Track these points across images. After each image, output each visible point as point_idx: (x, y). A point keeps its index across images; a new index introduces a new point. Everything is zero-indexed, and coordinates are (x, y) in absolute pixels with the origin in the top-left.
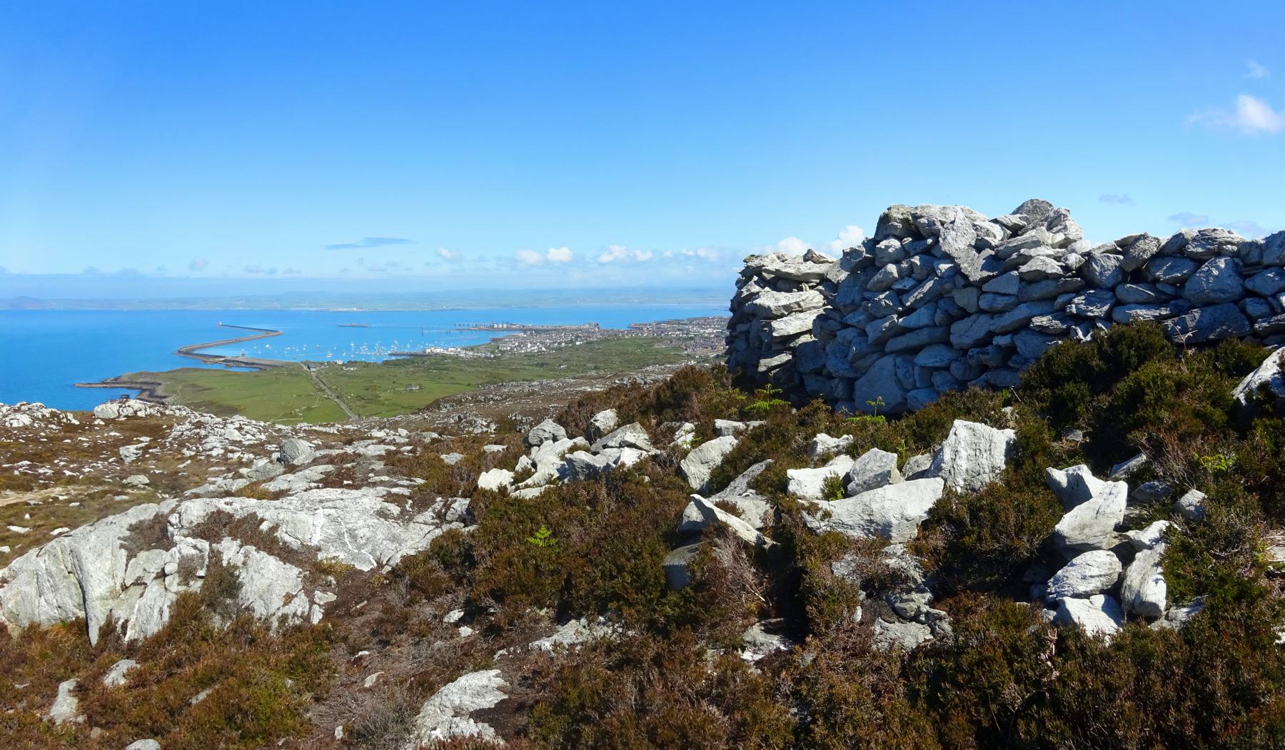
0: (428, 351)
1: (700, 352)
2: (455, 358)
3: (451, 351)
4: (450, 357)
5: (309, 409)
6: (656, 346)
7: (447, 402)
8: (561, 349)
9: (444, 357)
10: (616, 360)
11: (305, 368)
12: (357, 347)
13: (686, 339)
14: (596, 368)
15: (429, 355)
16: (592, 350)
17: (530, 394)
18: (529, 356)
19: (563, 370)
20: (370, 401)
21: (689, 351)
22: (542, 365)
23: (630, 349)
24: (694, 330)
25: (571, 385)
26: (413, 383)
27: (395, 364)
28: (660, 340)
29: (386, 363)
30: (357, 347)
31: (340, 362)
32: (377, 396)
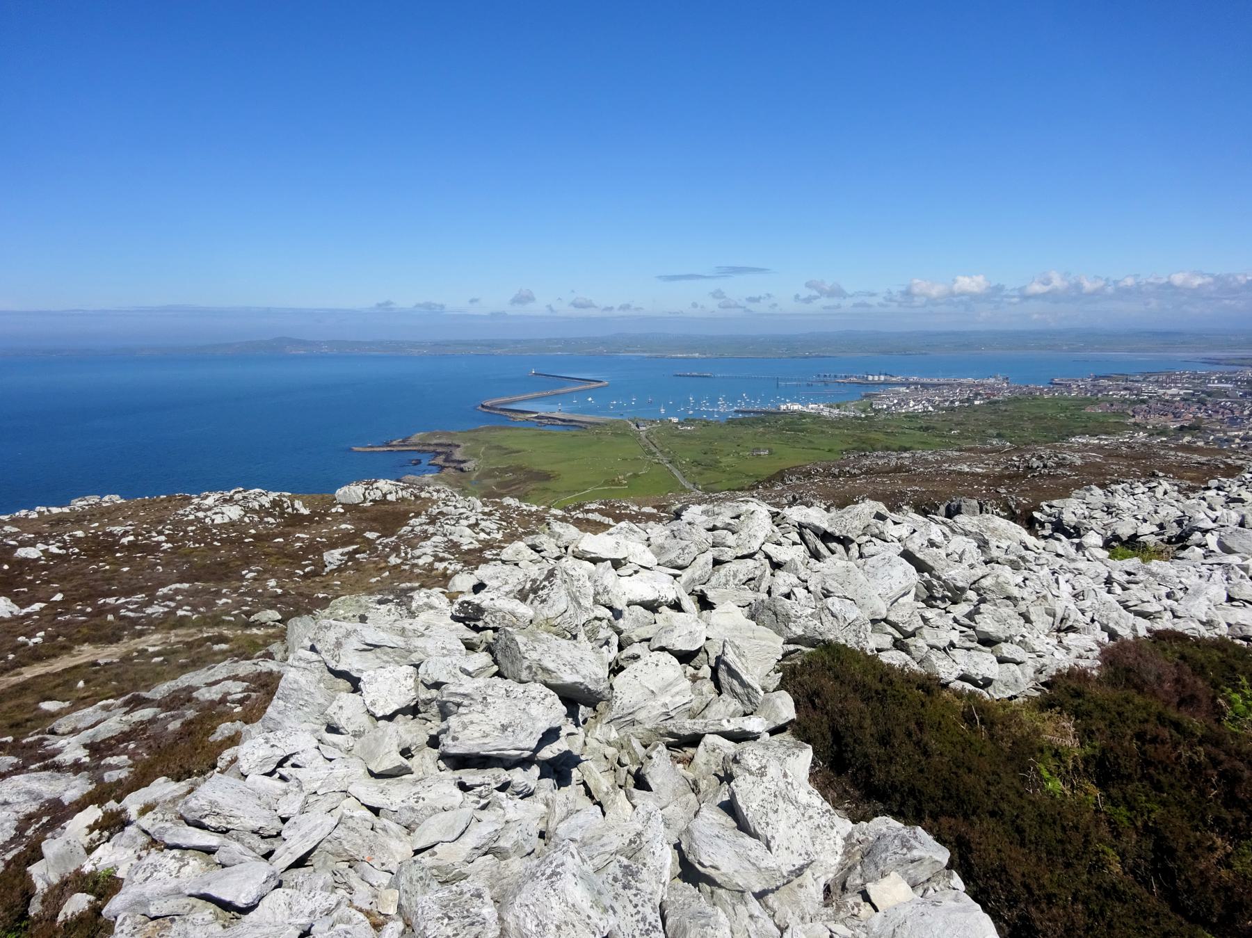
0: (783, 407)
1: (1154, 420)
2: (817, 418)
3: (812, 408)
4: (809, 415)
5: (635, 475)
6: (1088, 410)
7: (792, 474)
8: (953, 409)
9: (802, 415)
10: (1028, 425)
11: (634, 426)
12: (697, 402)
13: (1134, 402)
14: (999, 436)
15: (784, 413)
16: (995, 412)
17: (898, 469)
18: (911, 417)
19: (954, 437)
20: (708, 467)
21: (1138, 419)
22: (927, 429)
23: (1050, 412)
24: (1148, 389)
25: (951, 460)
26: (761, 446)
27: (741, 423)
28: (1096, 402)
29: (731, 422)
30: (697, 402)
31: (675, 420)
32: (718, 462)
